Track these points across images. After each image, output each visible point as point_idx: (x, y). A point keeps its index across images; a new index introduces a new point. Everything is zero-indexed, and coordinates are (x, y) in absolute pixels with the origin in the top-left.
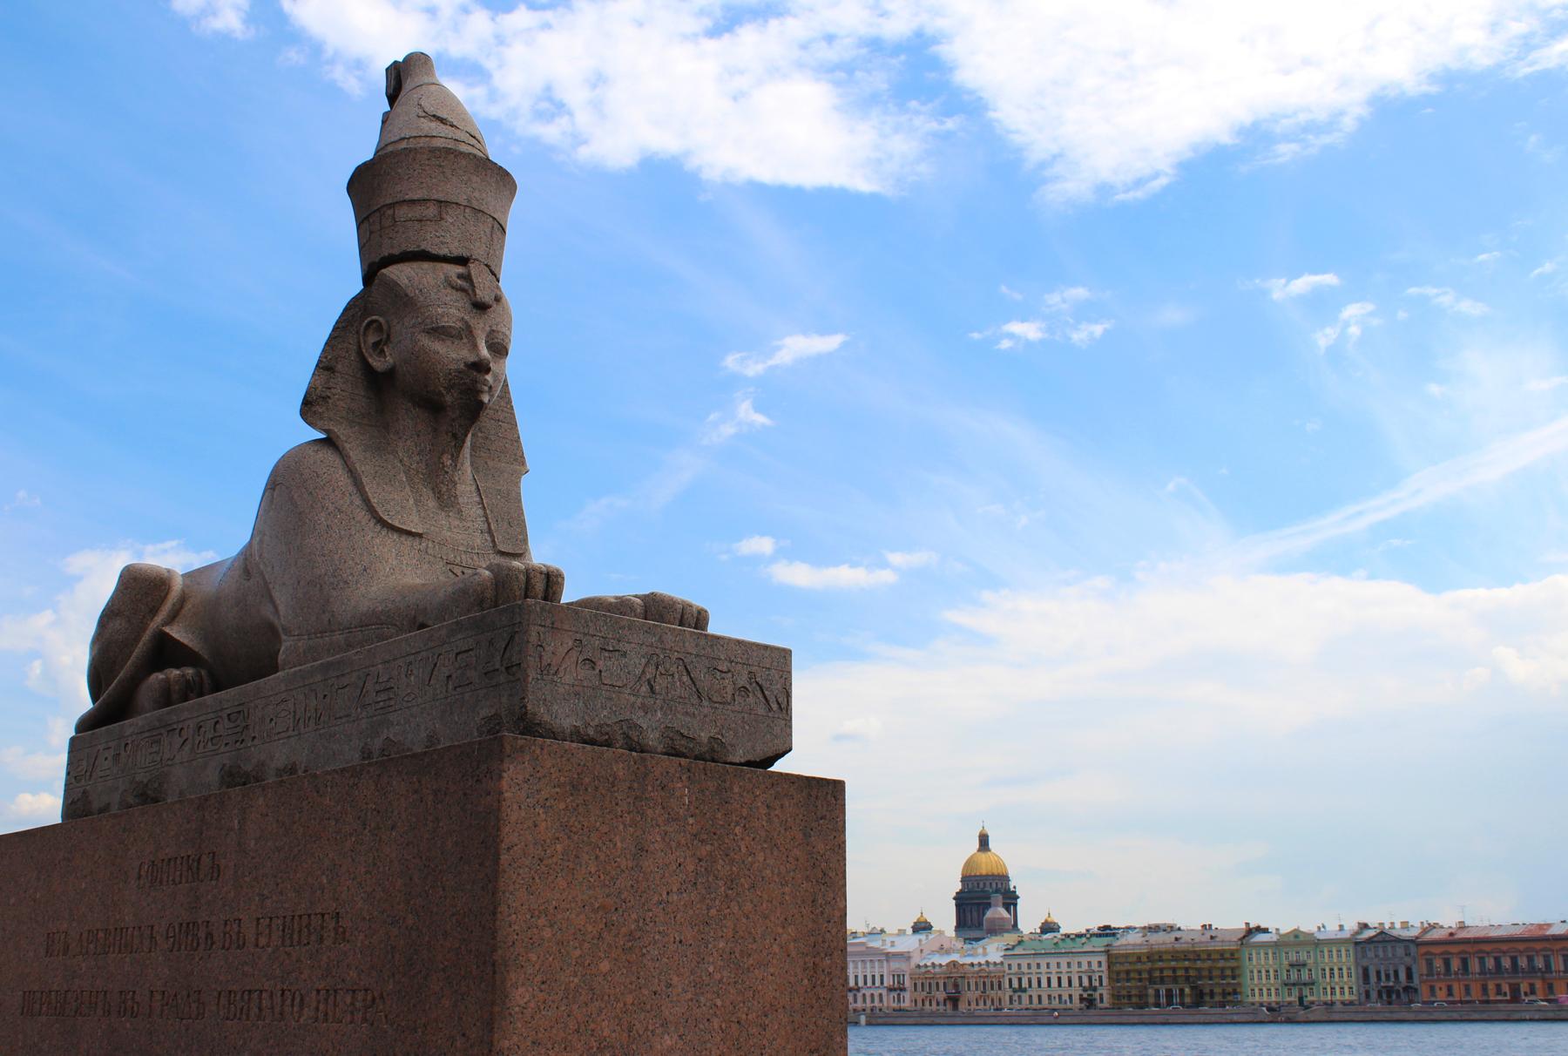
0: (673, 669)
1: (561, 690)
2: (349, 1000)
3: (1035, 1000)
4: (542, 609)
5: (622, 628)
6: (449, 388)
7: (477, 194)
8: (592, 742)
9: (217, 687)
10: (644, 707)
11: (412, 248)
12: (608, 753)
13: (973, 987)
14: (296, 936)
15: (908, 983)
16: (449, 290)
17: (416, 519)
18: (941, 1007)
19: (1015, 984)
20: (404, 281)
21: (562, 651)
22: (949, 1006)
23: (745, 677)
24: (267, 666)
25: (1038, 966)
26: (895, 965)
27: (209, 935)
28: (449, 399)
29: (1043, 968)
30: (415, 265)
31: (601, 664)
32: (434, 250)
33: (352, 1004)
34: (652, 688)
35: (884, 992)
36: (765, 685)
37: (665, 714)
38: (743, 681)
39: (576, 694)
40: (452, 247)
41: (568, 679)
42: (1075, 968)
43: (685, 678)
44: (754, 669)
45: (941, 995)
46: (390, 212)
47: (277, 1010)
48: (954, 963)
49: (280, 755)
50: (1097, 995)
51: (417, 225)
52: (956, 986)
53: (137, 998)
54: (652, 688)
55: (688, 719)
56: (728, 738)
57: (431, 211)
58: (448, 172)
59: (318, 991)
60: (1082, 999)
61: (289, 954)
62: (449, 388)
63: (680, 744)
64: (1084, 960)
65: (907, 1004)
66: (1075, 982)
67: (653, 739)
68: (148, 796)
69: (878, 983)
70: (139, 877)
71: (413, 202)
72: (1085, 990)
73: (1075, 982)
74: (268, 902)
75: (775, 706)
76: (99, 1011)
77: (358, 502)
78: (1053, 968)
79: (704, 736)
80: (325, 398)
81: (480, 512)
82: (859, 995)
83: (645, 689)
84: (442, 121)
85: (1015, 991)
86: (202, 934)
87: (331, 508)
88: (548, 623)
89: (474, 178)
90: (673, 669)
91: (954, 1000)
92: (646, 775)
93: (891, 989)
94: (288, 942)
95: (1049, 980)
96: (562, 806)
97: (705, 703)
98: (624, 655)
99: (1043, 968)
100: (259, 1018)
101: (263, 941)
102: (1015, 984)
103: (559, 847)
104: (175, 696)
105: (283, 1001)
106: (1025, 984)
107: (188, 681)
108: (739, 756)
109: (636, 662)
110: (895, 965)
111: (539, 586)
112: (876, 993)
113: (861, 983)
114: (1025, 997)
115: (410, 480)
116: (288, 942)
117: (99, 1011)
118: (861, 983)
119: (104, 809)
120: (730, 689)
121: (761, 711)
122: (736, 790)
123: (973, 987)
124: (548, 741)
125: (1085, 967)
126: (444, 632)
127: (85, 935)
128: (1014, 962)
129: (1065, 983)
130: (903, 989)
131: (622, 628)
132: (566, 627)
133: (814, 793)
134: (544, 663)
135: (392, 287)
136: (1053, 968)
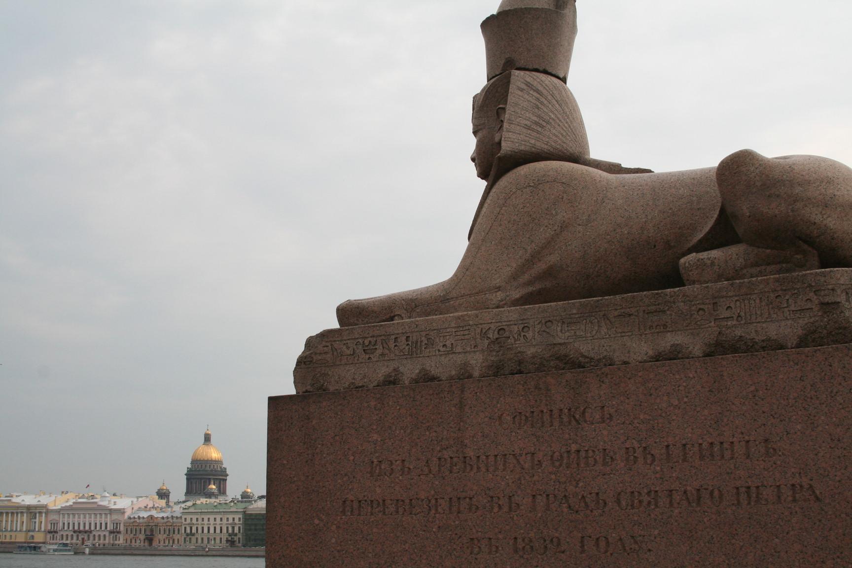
3: (200, 541)
13: (162, 532)
15: (122, 528)
18: (142, 544)
19: (188, 531)
22: (146, 544)
25: (203, 519)
26: (115, 517)
29: (206, 522)
35: (107, 534)
42: (225, 521)
45: (142, 537)
48: (151, 517)
50: (236, 539)
52: (152, 531)
60: (227, 541)
64: (231, 517)
65: (121, 541)
66: (224, 530)
69: (103, 528)
72: (230, 535)
73: (224, 530)
78: (212, 521)
82: (91, 536)
85: (188, 535)
91: (150, 540)
93: (111, 532)
95: (209, 528)
99: (206, 522)
102: (188, 531)
106: (194, 530)
110: (115, 517)
112: (102, 534)
113: (93, 528)
114: (194, 539)
118: (93, 528)
123: (162, 532)
125: (231, 521)
128: (188, 517)
129: (218, 531)
130: (119, 532)
136: (212, 521)
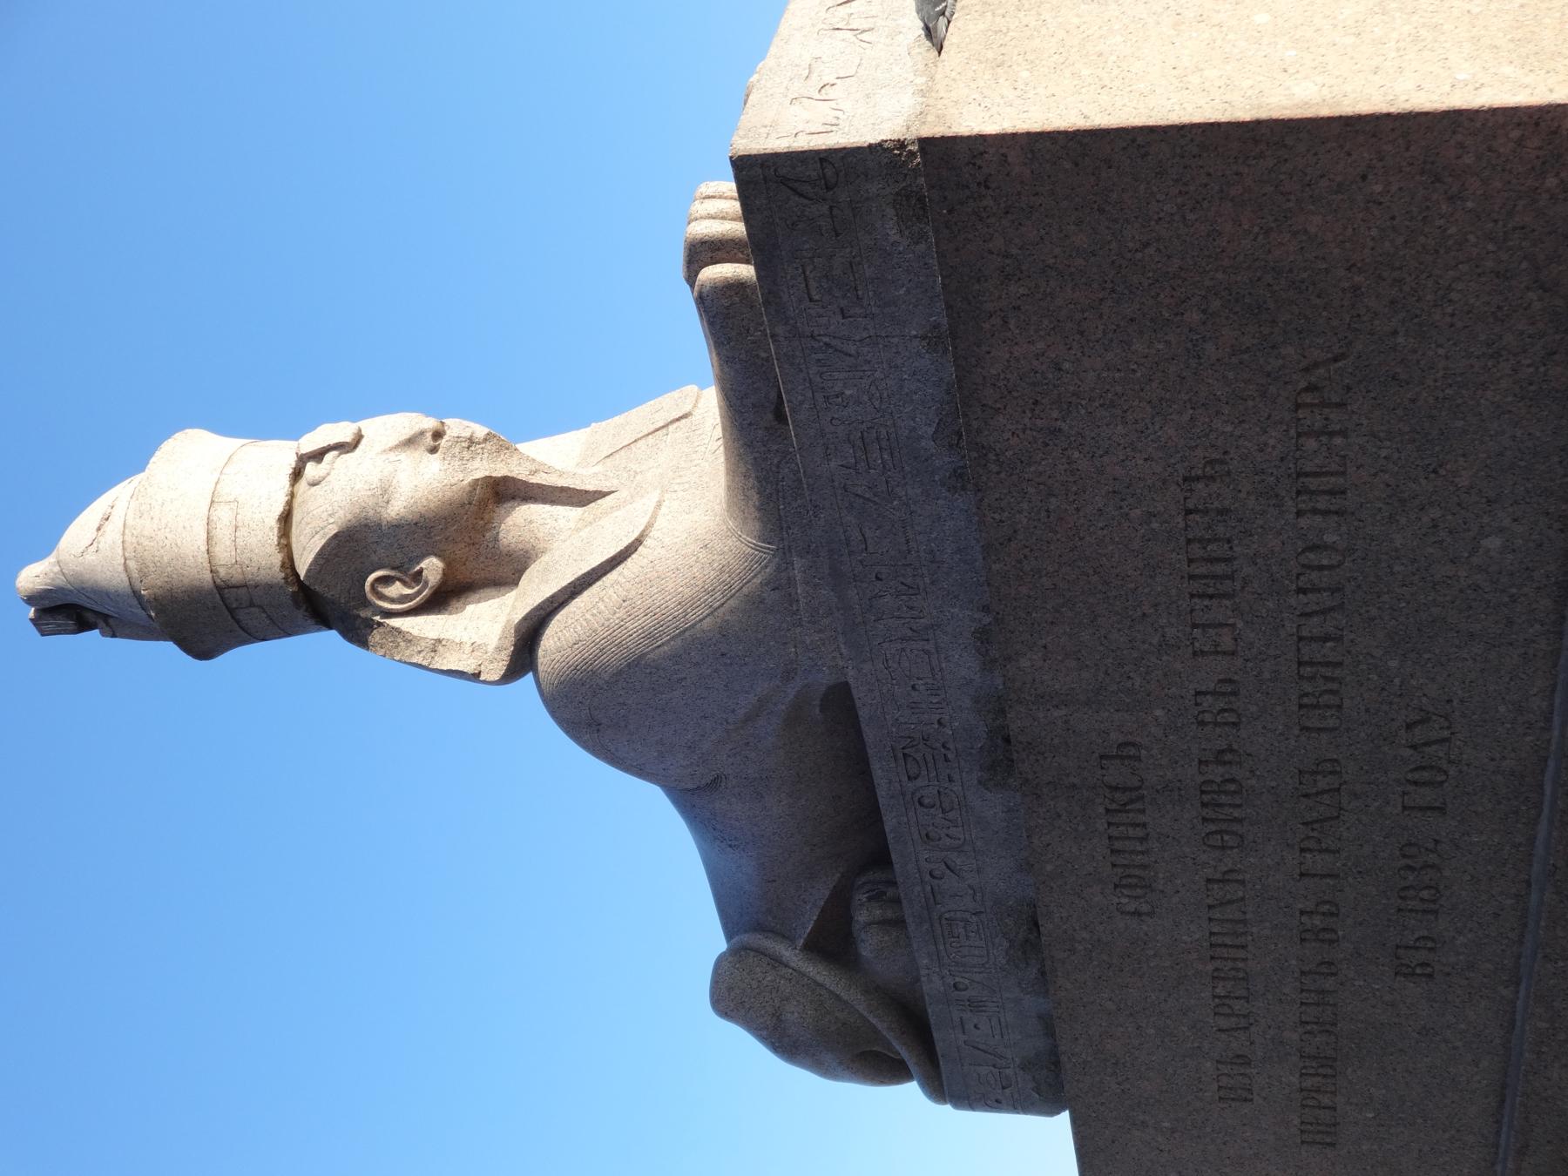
2: (1311, 444)
9: (880, 858)
11: (273, 537)
14: (1219, 569)
20: (318, 543)
24: (840, 699)
27: (1219, 757)
28: (479, 475)
30: (295, 531)
32: (279, 508)
33: (1317, 434)
46: (222, 572)
47: (1326, 599)
49: (963, 665)
51: (242, 532)
53: (1310, 906)
57: (223, 515)
59: (1299, 514)
61: (1246, 582)
68: (1028, 936)
70: (1137, 913)
74: (1171, 632)
76: (1329, 984)
77: (613, 576)
86: (1216, 773)
87: (621, 613)
94: (1227, 586)
96: (1025, 74)
100: (1339, 639)
101: (1227, 642)
103: (1085, 72)
104: (889, 914)
105: (1316, 590)
107: (870, 899)
116: (1227, 586)
117: (1329, 984)
119: (1048, 1025)
126: (780, 330)
127: (1223, 1023)
135: (326, 557)
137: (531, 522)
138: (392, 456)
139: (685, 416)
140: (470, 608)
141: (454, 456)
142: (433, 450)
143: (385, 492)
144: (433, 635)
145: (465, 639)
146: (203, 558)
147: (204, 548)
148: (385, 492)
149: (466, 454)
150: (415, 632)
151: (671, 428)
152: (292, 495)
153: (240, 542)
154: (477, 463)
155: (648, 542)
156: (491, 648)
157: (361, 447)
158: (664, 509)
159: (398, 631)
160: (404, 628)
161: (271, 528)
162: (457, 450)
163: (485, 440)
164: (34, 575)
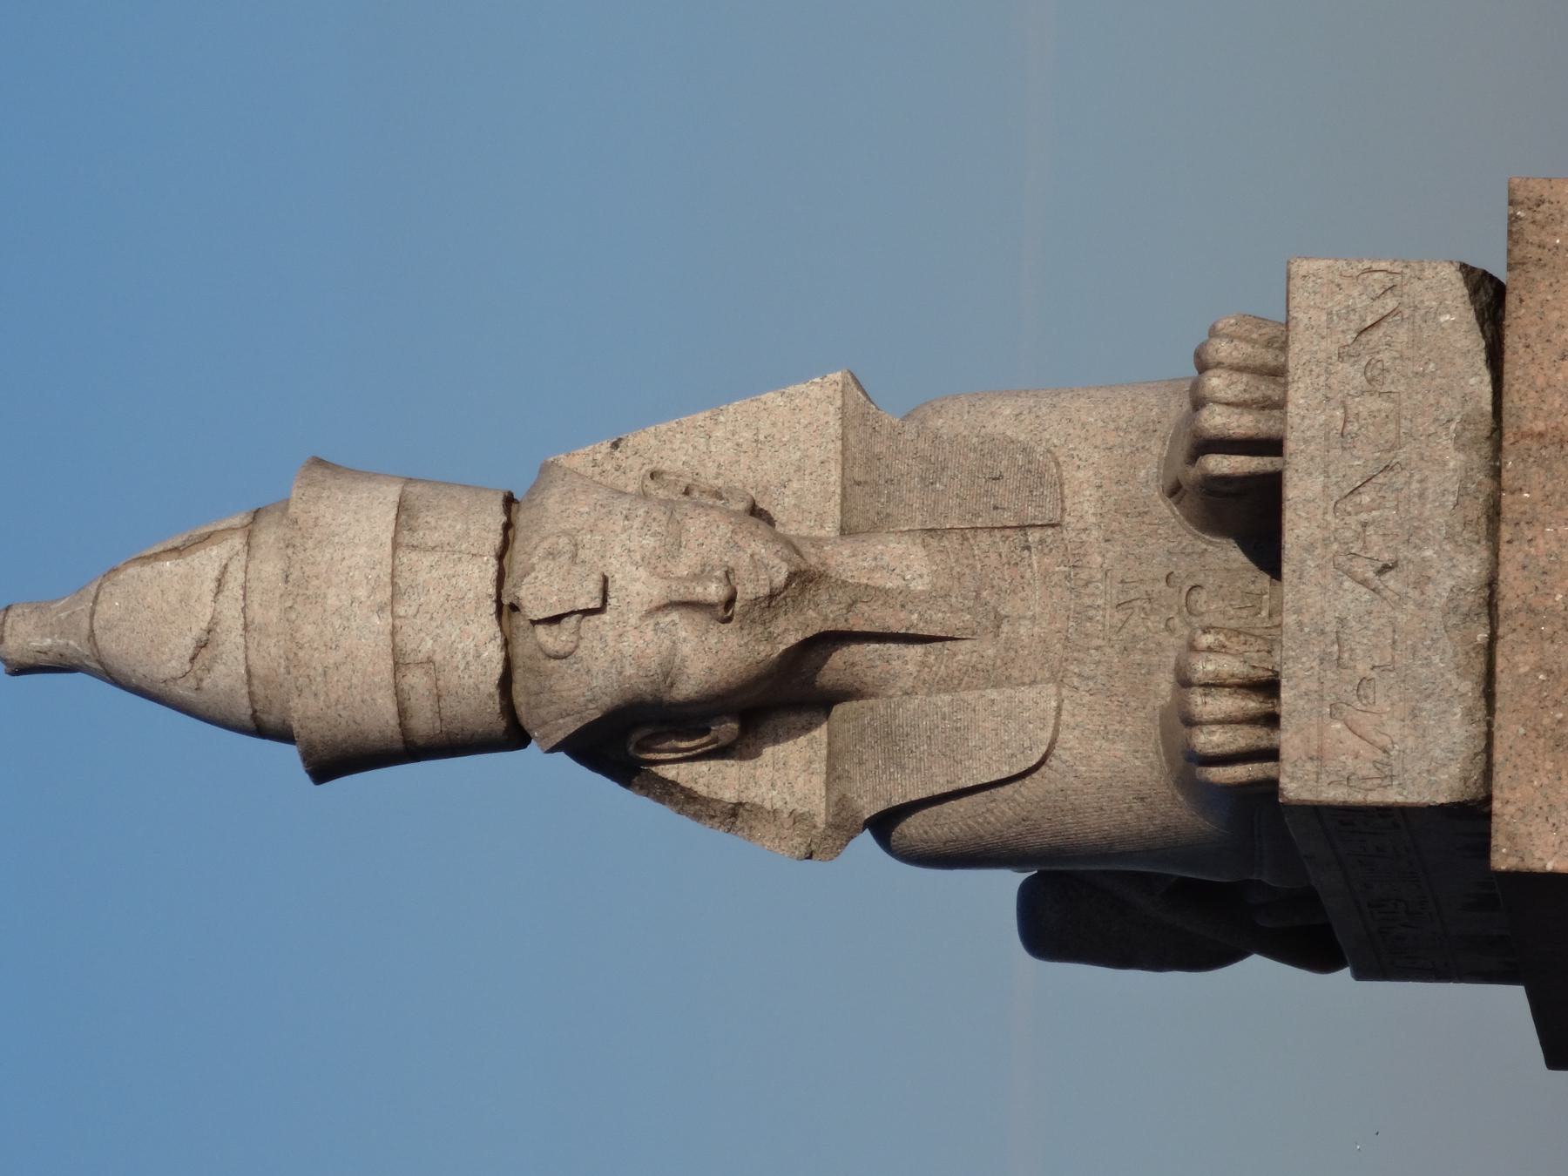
0: (1353, 521)
1: (1410, 742)
4: (1292, 778)
5: (1300, 624)
6: (770, 638)
7: (362, 593)
8: (1489, 694)
10: (1422, 581)
11: (495, 705)
12: (1503, 684)
16: (580, 653)
17: (1028, 694)
21: (1352, 742)
23: (1344, 368)
28: (792, 639)
31: (1362, 668)
32: (497, 670)
34: (1385, 569)
36: (1355, 324)
37: (1426, 540)
38: (1351, 373)
39: (1414, 714)
40: (482, 636)
41: (1393, 728)
43: (1366, 499)
44: (1334, 348)
54: (1385, 569)
55: (1430, 494)
56: (1450, 405)
57: (416, 680)
58: (333, 657)
62: (770, 638)
63: (1476, 509)
67: (1471, 568)
71: (402, 712)
75: (1391, 303)
77: (1007, 790)
79: (1455, 460)
80: (797, 818)
81: (984, 538)
83: (1391, 581)
84: (202, 645)
88: (1310, 766)
89: (332, 601)
90: (1353, 521)
92: (1531, 610)
97: (1401, 457)
98: (1342, 621)
108: (1481, 384)
109: (1352, 598)
111: (1225, 704)
115: (947, 684)
120: (1374, 403)
121: (1403, 335)
122: (1540, 426)
124: (1496, 793)
131: (1300, 624)
132: (1314, 731)
133: (1534, 252)
134: (1373, 773)
137: (853, 665)
138: (665, 619)
139: (1053, 526)
140: (768, 752)
141: (753, 621)
142: (729, 620)
143: (669, 673)
144: (729, 796)
145: (779, 805)
146: (398, 737)
147: (394, 722)
148: (669, 673)
149: (767, 615)
150: (701, 789)
151: (1034, 536)
152: (506, 644)
153: (447, 713)
154: (781, 624)
155: (1053, 762)
156: (820, 821)
157: (612, 602)
158: (1065, 717)
159: (674, 783)
160: (682, 781)
161: (490, 696)
162: (756, 614)
163: (786, 586)
164: (28, 635)
